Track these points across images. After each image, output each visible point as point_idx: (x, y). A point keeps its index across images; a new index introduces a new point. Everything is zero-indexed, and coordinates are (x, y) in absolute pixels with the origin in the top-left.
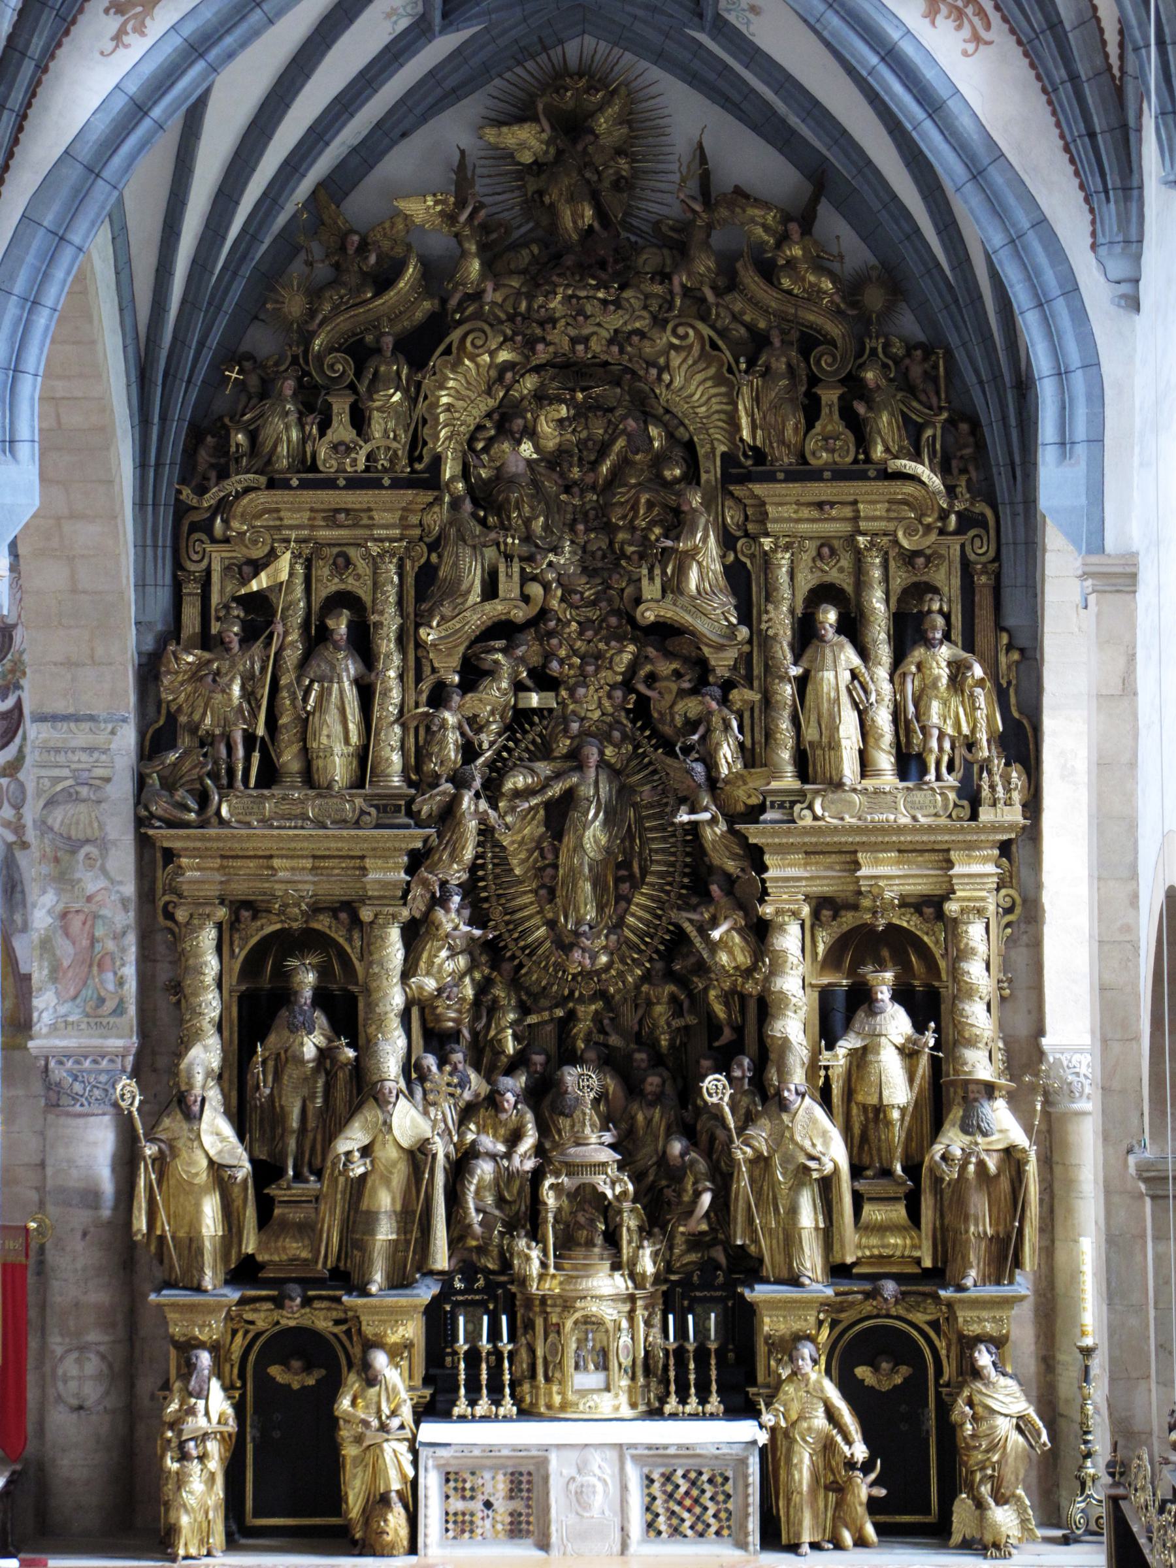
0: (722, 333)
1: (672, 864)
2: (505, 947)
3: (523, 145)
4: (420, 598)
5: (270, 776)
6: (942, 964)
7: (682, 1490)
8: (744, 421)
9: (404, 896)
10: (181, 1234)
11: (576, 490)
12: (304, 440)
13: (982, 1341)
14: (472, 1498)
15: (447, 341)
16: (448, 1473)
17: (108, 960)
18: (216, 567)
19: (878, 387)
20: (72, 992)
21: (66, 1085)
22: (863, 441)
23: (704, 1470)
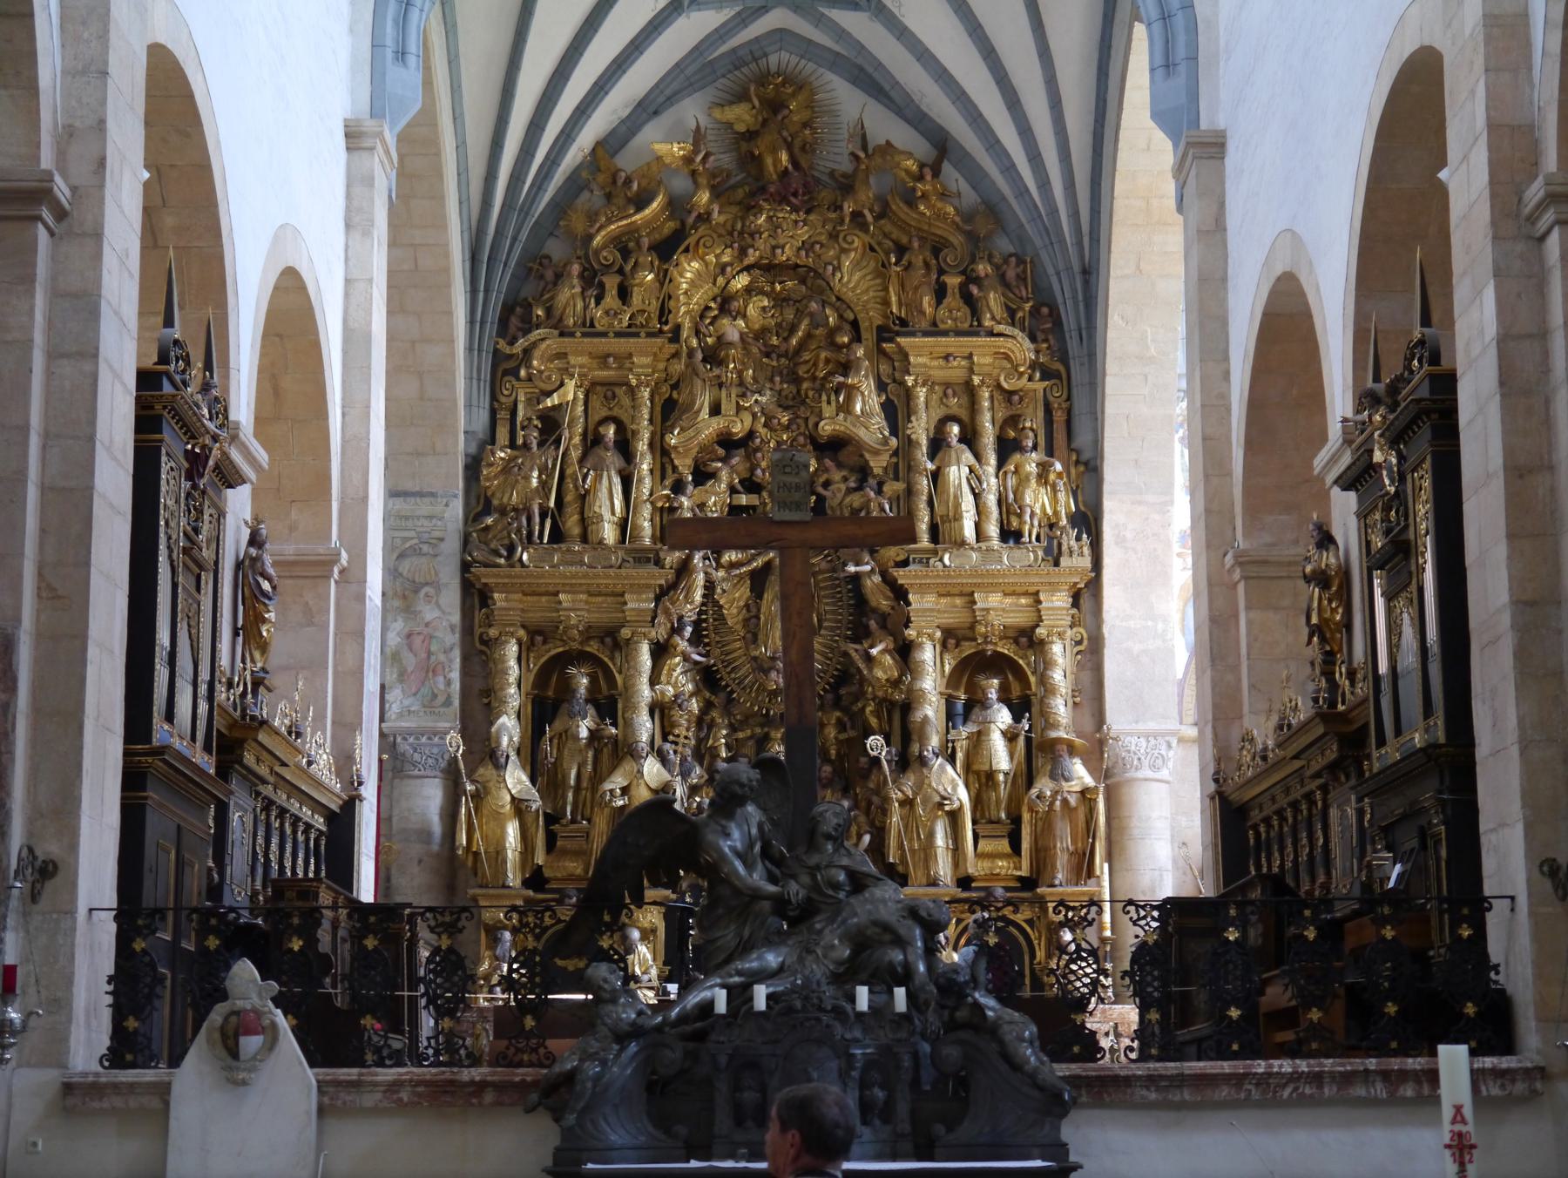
0: (879, 244)
1: (840, 621)
2: (721, 678)
3: (739, 119)
4: (665, 418)
5: (558, 536)
6: (1033, 679)
8: (894, 299)
9: (654, 618)
10: (491, 849)
11: (774, 356)
12: (586, 308)
15: (686, 243)
17: (440, 667)
18: (522, 398)
19: (987, 275)
20: (414, 690)
21: (408, 755)
22: (975, 313)
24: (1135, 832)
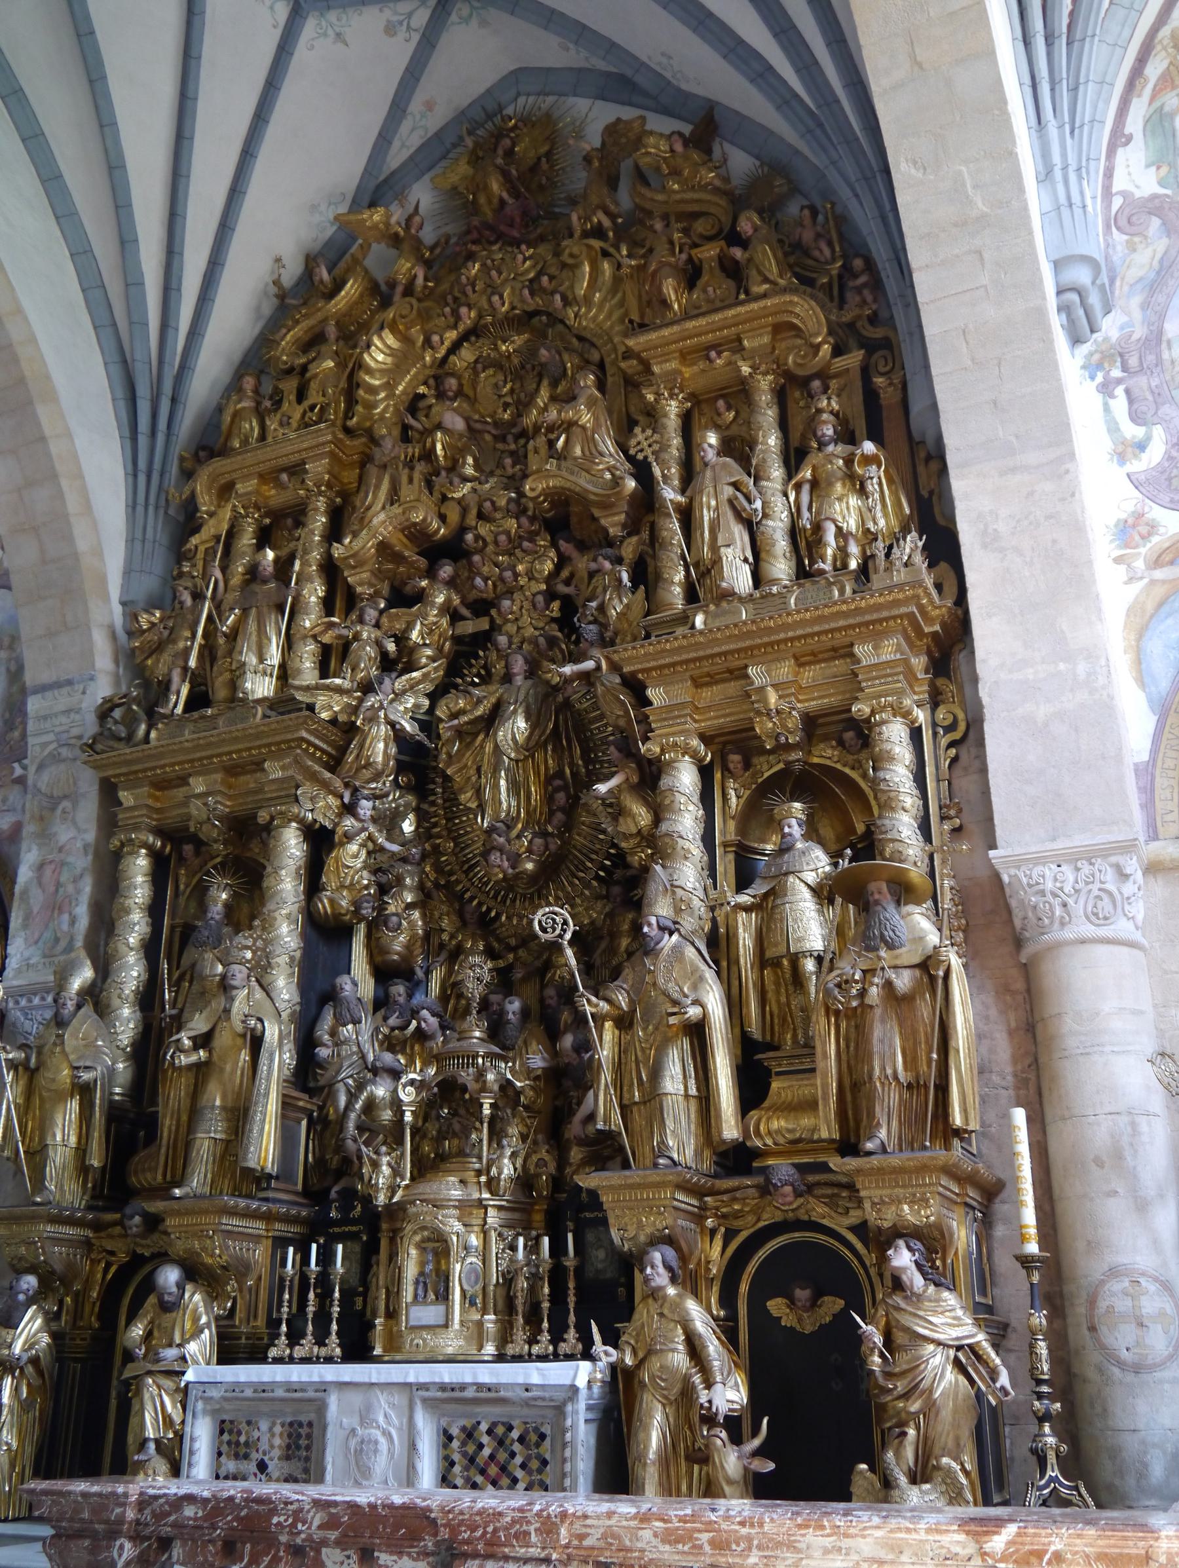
7: (486, 1452)
11: (510, 438)
13: (901, 1236)
14: (246, 1457)
16: (223, 1422)
20: (36, 936)
23: (515, 1423)
24: (1072, 1043)
